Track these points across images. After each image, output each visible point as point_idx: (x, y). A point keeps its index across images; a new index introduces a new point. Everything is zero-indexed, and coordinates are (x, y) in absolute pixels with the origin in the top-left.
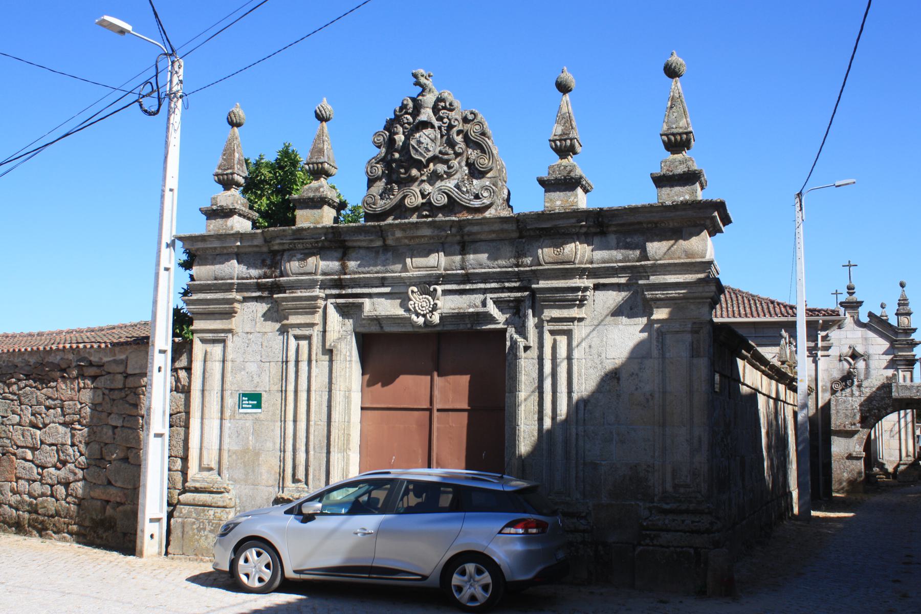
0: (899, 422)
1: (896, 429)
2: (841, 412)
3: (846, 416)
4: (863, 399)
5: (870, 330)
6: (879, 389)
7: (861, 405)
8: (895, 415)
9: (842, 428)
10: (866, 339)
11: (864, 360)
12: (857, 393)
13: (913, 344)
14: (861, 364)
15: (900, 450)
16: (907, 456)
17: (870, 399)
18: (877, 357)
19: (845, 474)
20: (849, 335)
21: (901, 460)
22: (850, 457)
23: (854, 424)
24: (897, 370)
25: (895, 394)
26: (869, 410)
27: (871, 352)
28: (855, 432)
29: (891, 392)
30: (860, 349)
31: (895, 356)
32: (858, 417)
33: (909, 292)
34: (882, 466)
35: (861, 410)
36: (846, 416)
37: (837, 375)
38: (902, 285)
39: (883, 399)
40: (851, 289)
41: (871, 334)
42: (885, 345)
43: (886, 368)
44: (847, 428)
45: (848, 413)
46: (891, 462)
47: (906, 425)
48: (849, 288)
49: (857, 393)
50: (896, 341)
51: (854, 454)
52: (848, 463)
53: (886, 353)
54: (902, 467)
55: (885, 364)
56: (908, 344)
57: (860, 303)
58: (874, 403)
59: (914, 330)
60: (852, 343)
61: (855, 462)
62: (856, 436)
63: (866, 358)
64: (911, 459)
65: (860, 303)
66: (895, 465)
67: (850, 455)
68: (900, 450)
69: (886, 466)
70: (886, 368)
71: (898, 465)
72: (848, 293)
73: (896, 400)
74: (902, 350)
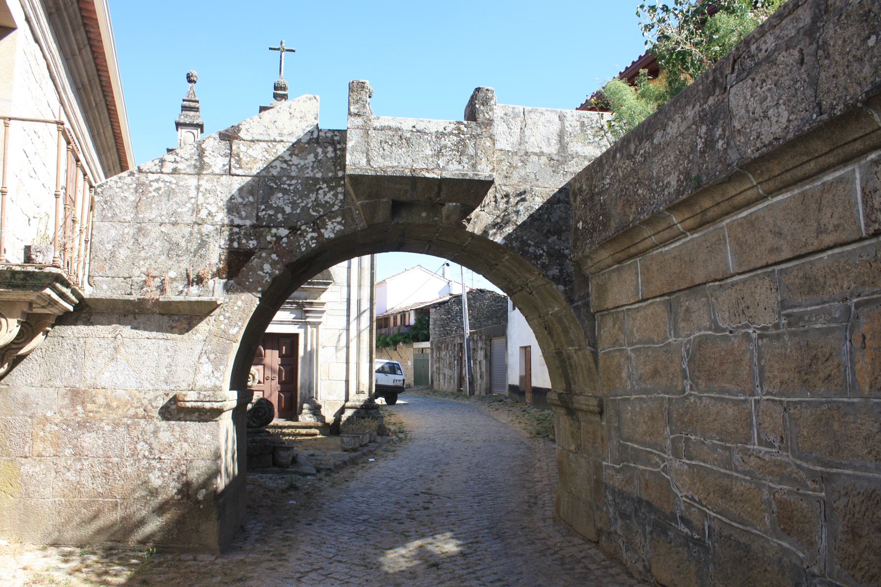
0: (348, 330)
1: (343, 342)
2: (154, 231)
3: (172, 249)
4: (237, 183)
6: (297, 148)
7: (232, 208)
8: (345, 264)
9: (151, 293)
12: (216, 162)
15: (347, 381)
16: (359, 392)
17: (263, 186)
19: (156, 481)
21: (347, 400)
22: (174, 410)
23: (200, 280)
25: (356, 161)
26: (258, 228)
28: (205, 309)
29: (339, 161)
32: (215, 254)
34: (316, 410)
35: (232, 225)
36: (172, 249)
39: (311, 185)
44: (171, 296)
45: (179, 234)
46: (331, 404)
47: (359, 335)
49: (216, 162)
51: (191, 399)
52: (168, 431)
54: (349, 413)
58: (278, 199)
61: (192, 428)
62: (203, 327)
64: (365, 397)
66: (338, 408)
67: (175, 399)
68: (347, 381)
69: (323, 412)
71: (342, 410)
72: (276, 96)
73: (357, 180)
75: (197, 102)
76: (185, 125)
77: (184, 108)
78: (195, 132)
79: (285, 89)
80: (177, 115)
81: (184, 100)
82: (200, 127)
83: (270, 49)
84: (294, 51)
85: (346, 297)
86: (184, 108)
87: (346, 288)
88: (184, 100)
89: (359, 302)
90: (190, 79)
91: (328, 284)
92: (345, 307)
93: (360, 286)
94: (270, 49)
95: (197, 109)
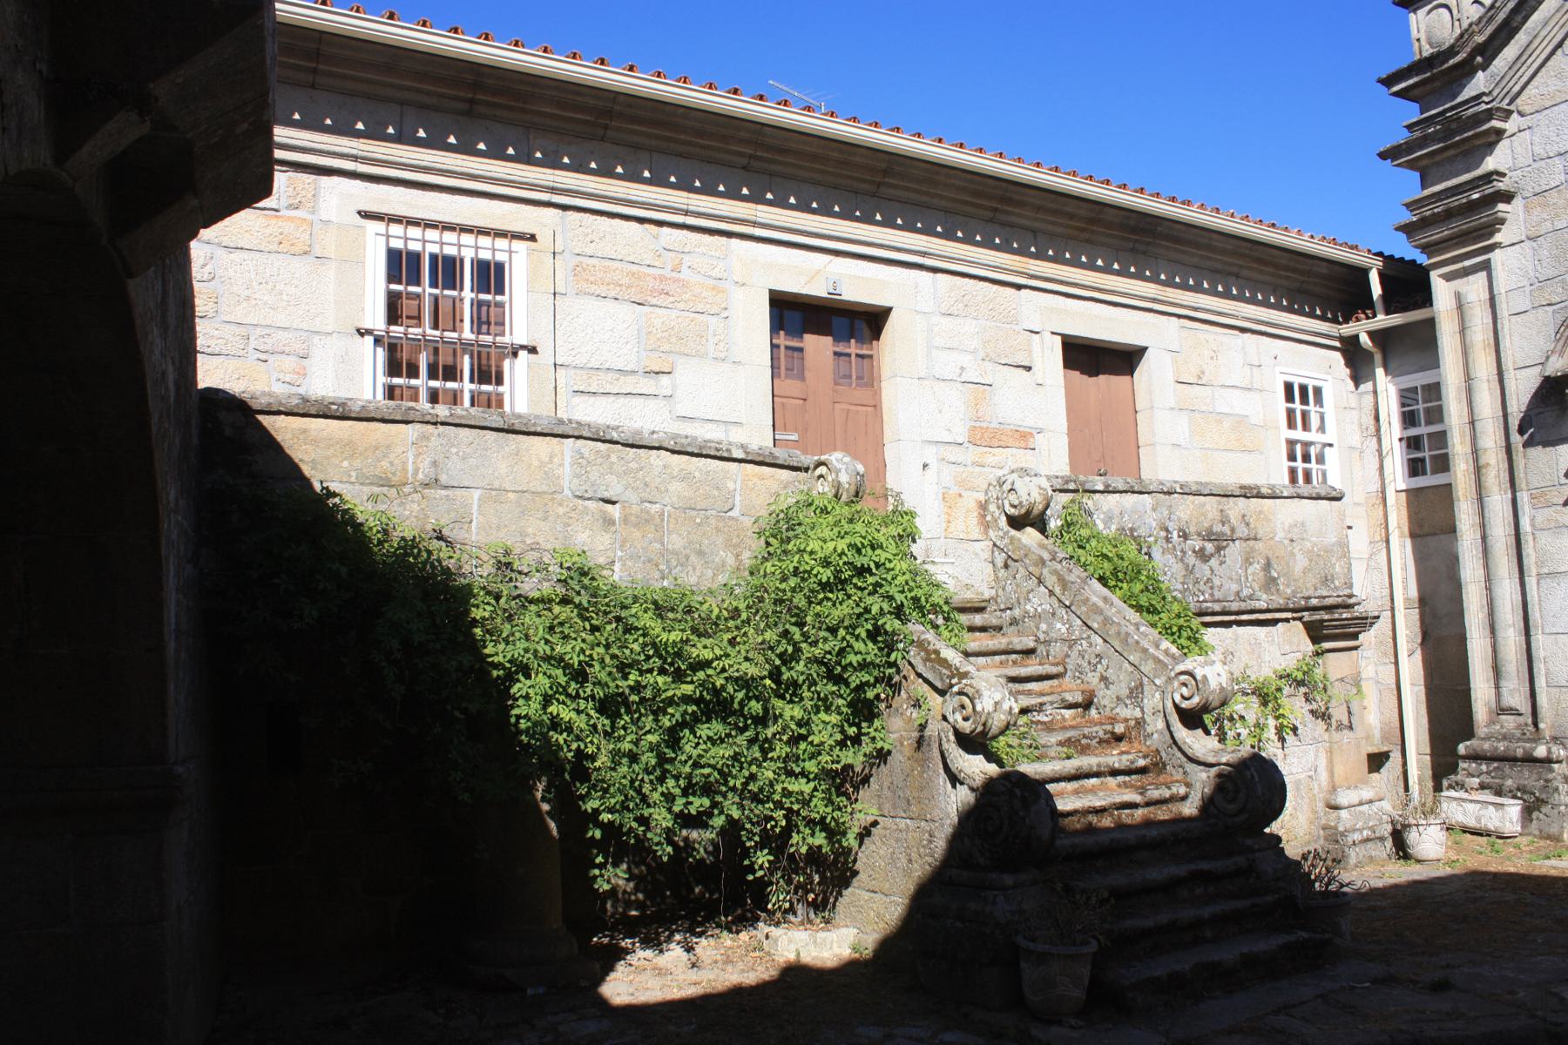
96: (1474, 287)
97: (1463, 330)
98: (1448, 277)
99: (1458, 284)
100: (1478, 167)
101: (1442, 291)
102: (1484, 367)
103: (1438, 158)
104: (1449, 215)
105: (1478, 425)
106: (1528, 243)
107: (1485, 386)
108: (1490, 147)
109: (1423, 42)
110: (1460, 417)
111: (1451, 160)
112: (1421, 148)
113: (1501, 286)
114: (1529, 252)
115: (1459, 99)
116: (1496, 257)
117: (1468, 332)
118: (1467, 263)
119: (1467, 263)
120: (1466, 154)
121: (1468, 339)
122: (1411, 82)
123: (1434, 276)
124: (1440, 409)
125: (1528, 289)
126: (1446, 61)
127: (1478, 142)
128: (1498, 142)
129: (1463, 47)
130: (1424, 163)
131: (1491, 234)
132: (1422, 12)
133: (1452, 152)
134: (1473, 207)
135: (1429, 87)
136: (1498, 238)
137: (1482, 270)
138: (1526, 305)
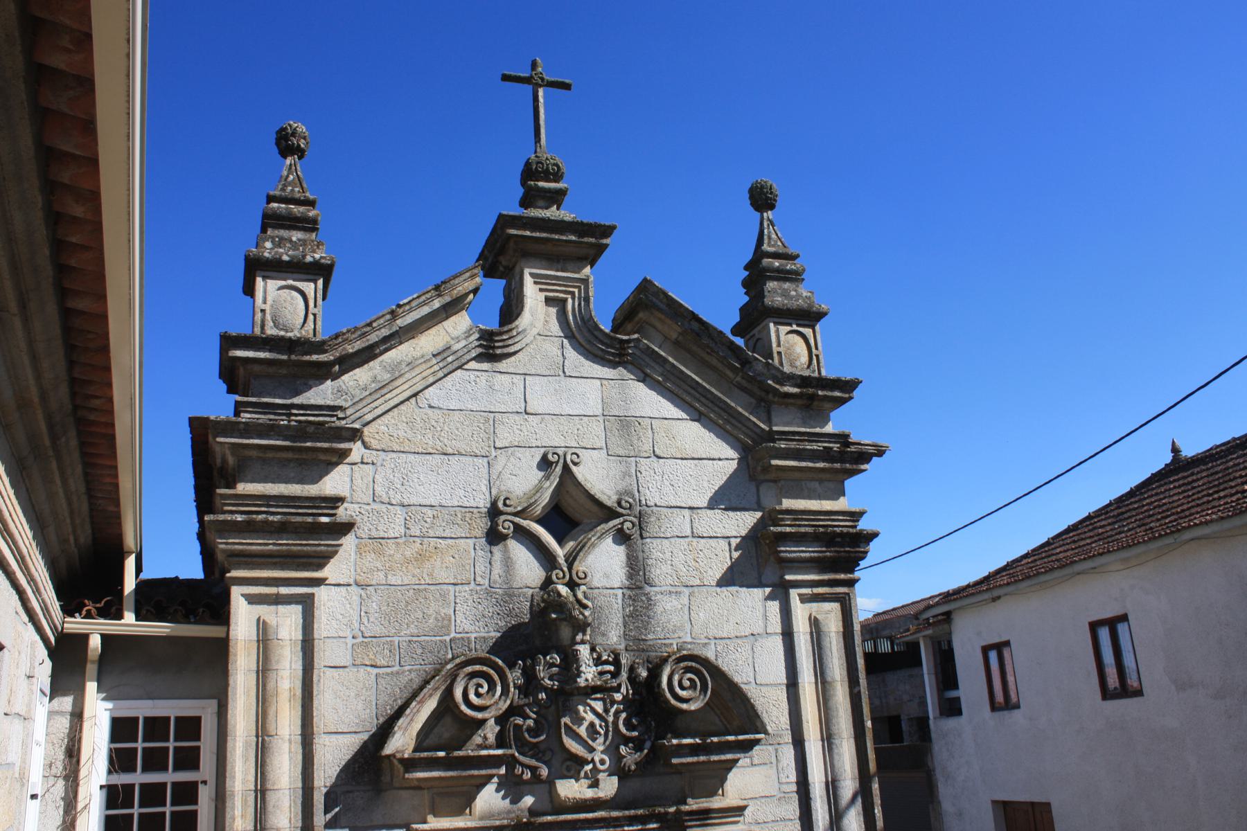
5: (645, 378)
10: (625, 424)
11: (622, 537)
13: (850, 457)
14: (604, 562)
18: (681, 523)
20: (542, 396)
24: (781, 591)
27: (652, 495)
30: (599, 477)
31: (772, 517)
33: (783, 230)
37: (475, 625)
38: (762, 199)
40: (538, 181)
41: (648, 402)
42: (718, 459)
43: (730, 579)
48: (530, 172)
50: (771, 436)
53: (725, 499)
55: (720, 558)
56: (826, 455)
57: (587, 242)
59: (849, 386)
60: (555, 437)
63: (627, 522)
65: (587, 242)
70: (730, 579)
74: (797, 484)
75: (312, 203)
76: (275, 268)
77: (270, 221)
78: (309, 288)
79: (557, 177)
80: (246, 238)
81: (270, 199)
82: (321, 271)
83: (506, 78)
84: (566, 86)
85: (793, 777)
86: (270, 221)
87: (788, 754)
88: (270, 199)
89: (832, 786)
90: (286, 145)
91: (747, 746)
92: (792, 809)
93: (828, 739)
94: (506, 78)
95: (310, 225)
96: (287, 622)
97: (264, 670)
98: (252, 600)
99: (264, 611)
100: (315, 481)
101: (244, 617)
102: (286, 722)
103: (270, 455)
104: (282, 529)
105: (271, 798)
106: (354, 588)
107: (286, 746)
108: (330, 466)
109: (268, 317)
110: (244, 781)
111: (284, 463)
112: (260, 437)
113: (323, 627)
114: (356, 599)
115: (297, 400)
116: (321, 593)
117: (272, 675)
118: (284, 590)
119: (284, 590)
120: (302, 463)
121: (271, 685)
122: (261, 355)
123: (236, 592)
124: (114, 738)
125: (350, 641)
126: (310, 354)
127: (322, 457)
128: (337, 464)
129: (333, 348)
130: (254, 453)
131: (320, 566)
132: (273, 285)
133: (290, 455)
134: (316, 530)
135: (271, 370)
136: (326, 572)
137: (297, 603)
138: (345, 659)
